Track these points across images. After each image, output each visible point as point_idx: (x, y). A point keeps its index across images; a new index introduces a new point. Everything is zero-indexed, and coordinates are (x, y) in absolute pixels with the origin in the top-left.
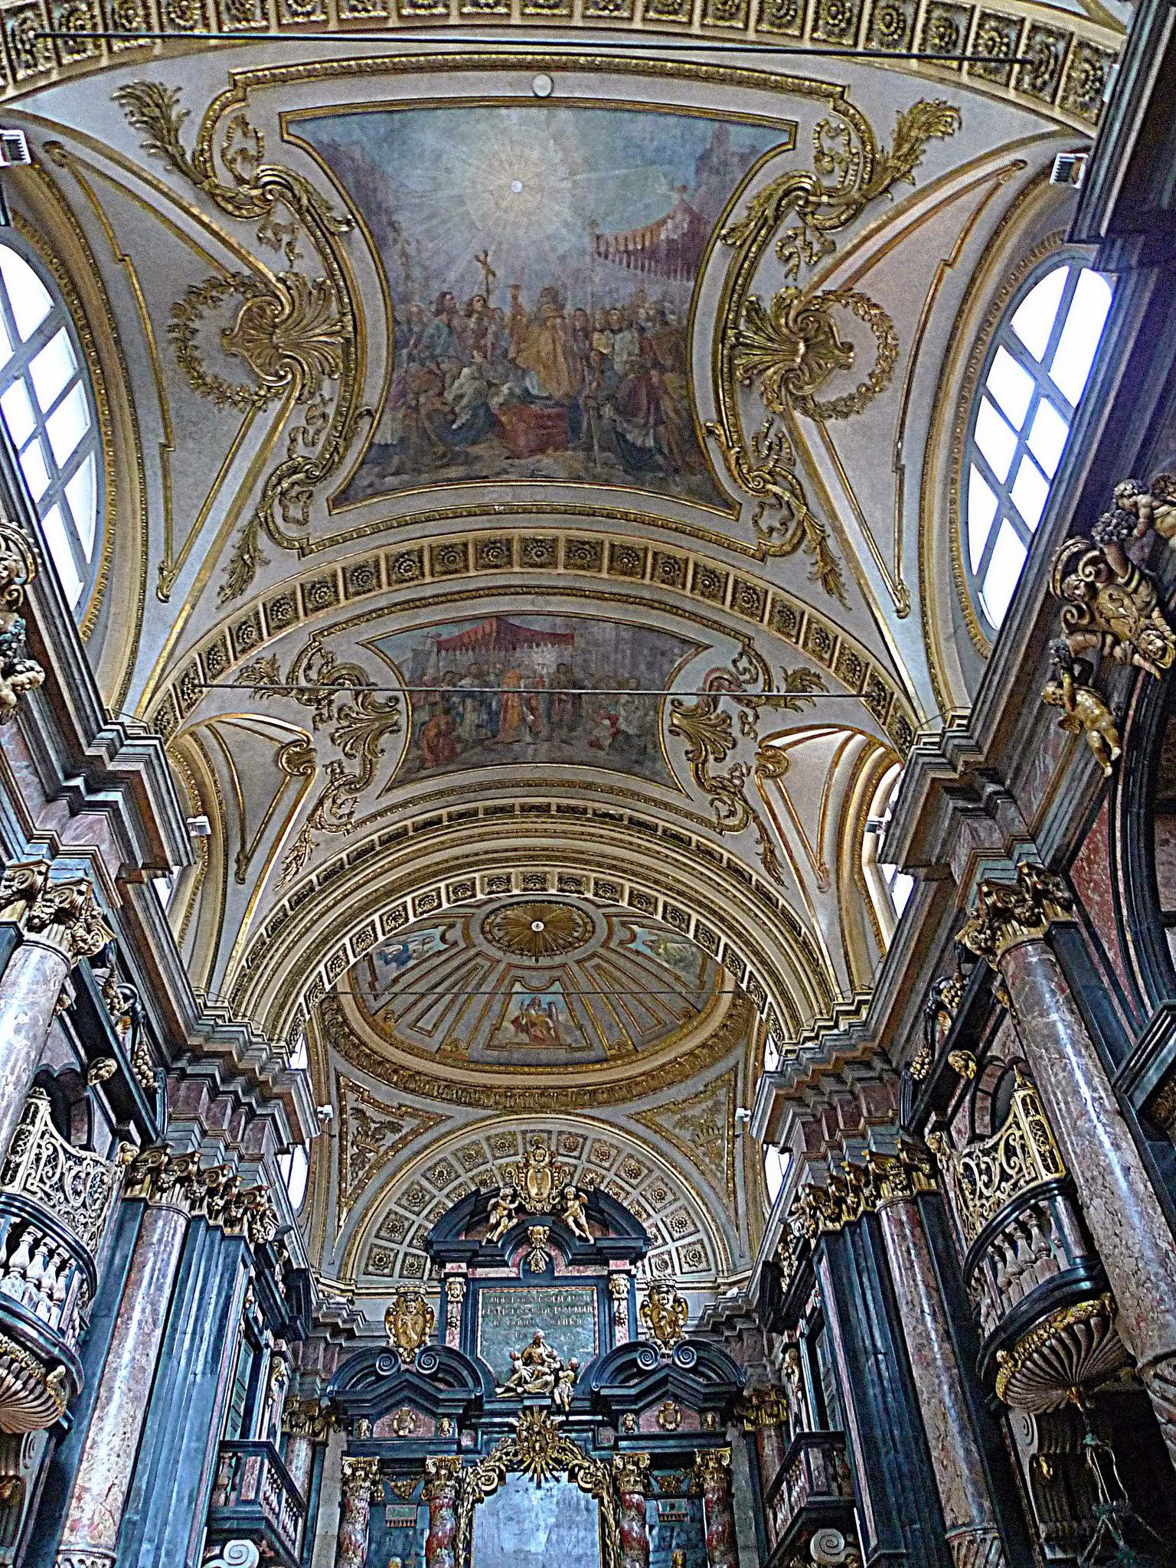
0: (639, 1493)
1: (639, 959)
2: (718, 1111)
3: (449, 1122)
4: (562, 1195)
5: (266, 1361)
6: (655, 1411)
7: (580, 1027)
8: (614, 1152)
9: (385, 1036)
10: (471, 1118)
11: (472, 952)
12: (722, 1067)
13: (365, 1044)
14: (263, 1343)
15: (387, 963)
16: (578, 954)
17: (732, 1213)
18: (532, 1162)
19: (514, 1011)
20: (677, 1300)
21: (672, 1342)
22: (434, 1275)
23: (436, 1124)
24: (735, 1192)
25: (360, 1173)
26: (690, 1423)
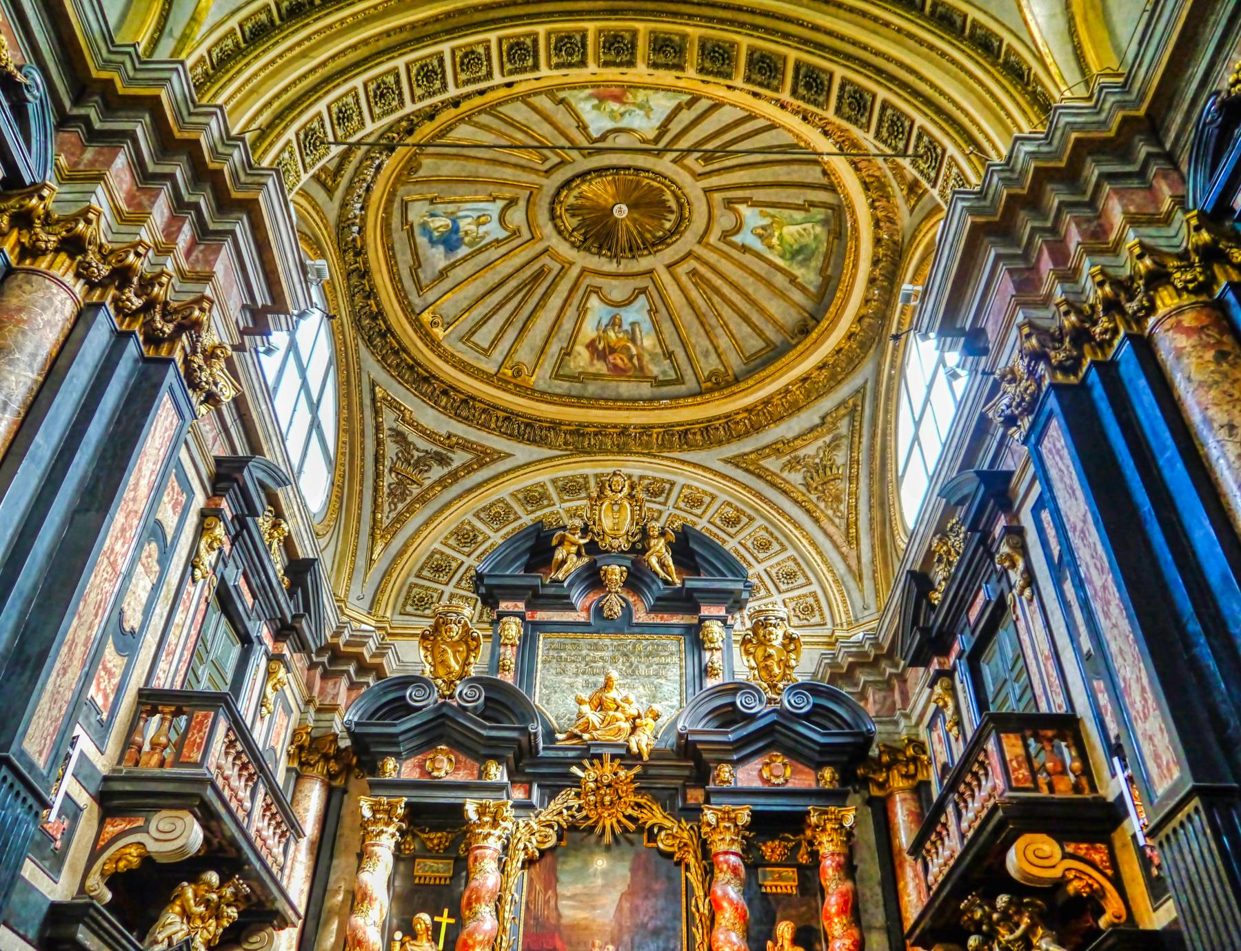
0: (733, 853)
1: (747, 259)
2: (838, 446)
3: (508, 460)
4: (645, 533)
5: (258, 663)
6: (756, 764)
7: (669, 355)
8: (707, 499)
9: (433, 344)
10: (535, 457)
11: (539, 247)
12: (844, 391)
13: (405, 350)
14: (253, 635)
15: (433, 243)
16: (669, 254)
17: (854, 563)
18: (609, 493)
19: (589, 330)
20: (790, 639)
21: (781, 685)
22: (485, 618)
23: (493, 461)
24: (857, 539)
25: (400, 506)
26: (804, 780)
